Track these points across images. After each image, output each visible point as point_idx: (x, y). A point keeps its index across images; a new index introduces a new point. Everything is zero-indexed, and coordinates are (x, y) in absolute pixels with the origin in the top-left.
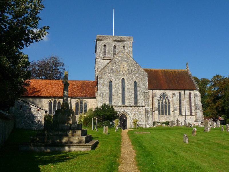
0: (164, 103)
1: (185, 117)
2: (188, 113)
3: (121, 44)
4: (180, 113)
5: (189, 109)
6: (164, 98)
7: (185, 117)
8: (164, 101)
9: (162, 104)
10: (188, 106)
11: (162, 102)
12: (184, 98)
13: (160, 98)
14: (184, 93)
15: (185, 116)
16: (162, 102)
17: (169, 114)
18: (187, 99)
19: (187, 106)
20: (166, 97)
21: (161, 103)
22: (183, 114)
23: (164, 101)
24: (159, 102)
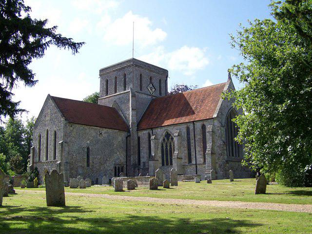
0: (168, 148)
1: (196, 167)
2: (200, 160)
3: (121, 73)
4: (190, 161)
5: (202, 153)
6: (168, 139)
7: (196, 167)
8: (169, 145)
9: (167, 148)
10: (200, 147)
11: (166, 146)
12: (193, 135)
13: (164, 140)
14: (194, 127)
15: (196, 164)
16: (166, 146)
17: (171, 164)
18: (199, 137)
19: (198, 149)
20: (170, 137)
21: (165, 148)
22: (194, 162)
23: (169, 145)
24: (162, 147)
